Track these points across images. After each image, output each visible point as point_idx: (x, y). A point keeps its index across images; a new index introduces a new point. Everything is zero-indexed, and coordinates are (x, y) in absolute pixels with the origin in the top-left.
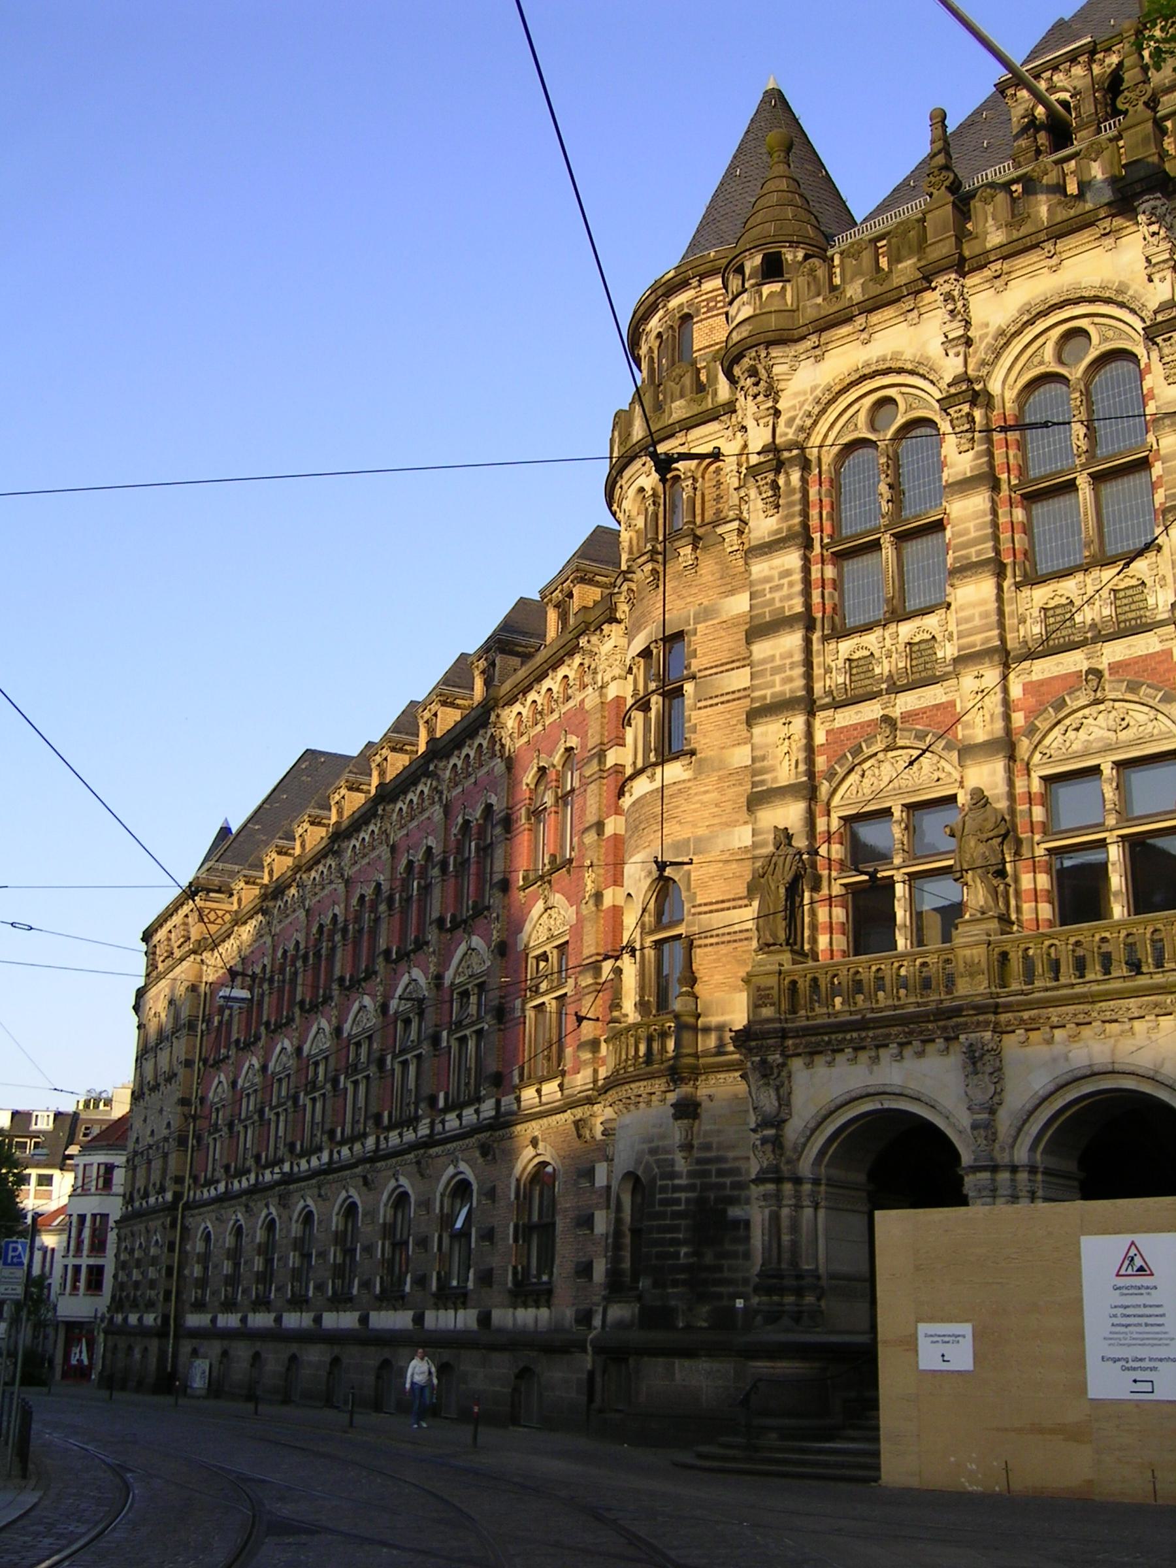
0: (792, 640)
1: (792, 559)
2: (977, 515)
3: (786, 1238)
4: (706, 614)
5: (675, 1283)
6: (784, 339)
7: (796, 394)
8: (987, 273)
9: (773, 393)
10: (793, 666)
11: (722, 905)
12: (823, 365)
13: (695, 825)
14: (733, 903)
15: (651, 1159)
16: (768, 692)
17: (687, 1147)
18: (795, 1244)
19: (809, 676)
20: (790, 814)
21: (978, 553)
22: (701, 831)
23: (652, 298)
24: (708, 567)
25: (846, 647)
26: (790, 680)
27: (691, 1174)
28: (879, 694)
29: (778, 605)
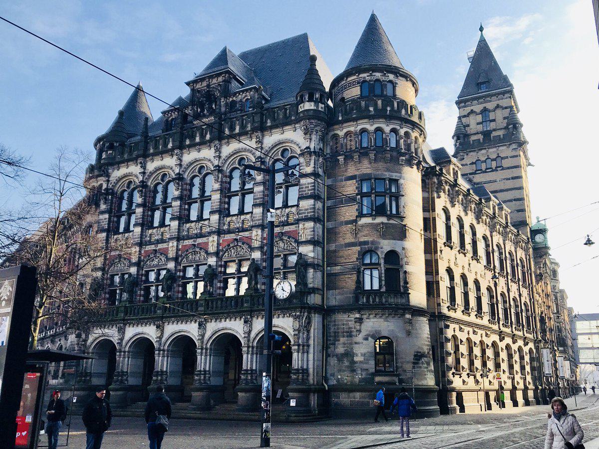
0: (104, 234)
1: (107, 216)
6: (112, 164)
7: (113, 177)
9: (108, 176)
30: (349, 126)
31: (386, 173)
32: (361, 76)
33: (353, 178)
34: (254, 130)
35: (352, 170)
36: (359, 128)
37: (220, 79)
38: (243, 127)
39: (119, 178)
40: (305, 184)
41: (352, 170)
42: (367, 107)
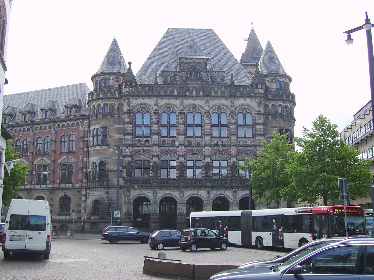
1: (131, 126)
2: (156, 128)
3: (129, 210)
4: (111, 126)
5: (105, 214)
6: (133, 96)
7: (133, 103)
8: (160, 97)
9: (130, 102)
10: (130, 140)
11: (112, 166)
12: (137, 101)
13: (108, 155)
14: (115, 166)
15: (101, 198)
16: (127, 143)
17: (107, 197)
18: (130, 210)
19: (132, 142)
20: (129, 159)
21: (156, 132)
22: (109, 156)
23: (103, 74)
24: (112, 120)
25: (137, 139)
26: (130, 142)
27: (107, 201)
28: (142, 146)
29: (129, 131)
30: (274, 102)
31: (289, 127)
32: (276, 78)
33: (276, 127)
34: (230, 96)
35: (275, 123)
36: (279, 104)
37: (201, 61)
38: (223, 93)
39: (137, 104)
40: (259, 128)
41: (275, 123)
42: (282, 95)
